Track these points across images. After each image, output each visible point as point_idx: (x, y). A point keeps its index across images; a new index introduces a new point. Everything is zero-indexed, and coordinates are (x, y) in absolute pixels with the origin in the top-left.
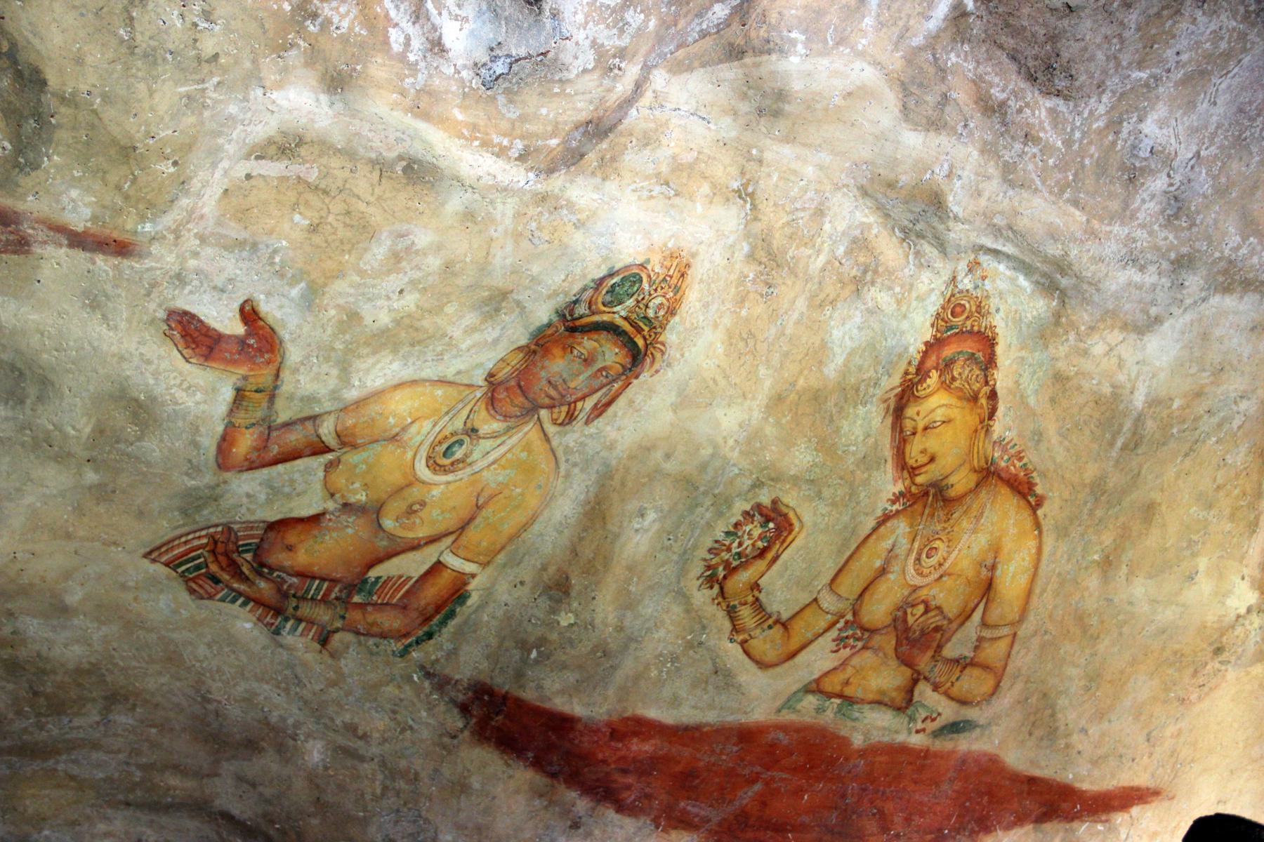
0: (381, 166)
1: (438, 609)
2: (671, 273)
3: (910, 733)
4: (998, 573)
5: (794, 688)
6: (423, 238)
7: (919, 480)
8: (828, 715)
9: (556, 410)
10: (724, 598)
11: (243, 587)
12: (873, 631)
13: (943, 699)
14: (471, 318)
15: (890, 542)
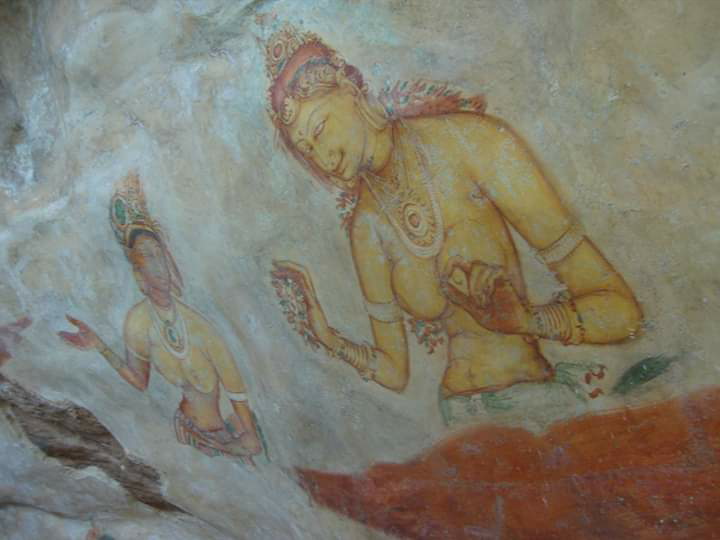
0: (35, 237)
3: (584, 400)
4: (493, 194)
5: (435, 397)
7: (348, 174)
8: (484, 417)
10: (331, 349)
12: (439, 318)
13: (587, 348)
15: (374, 235)
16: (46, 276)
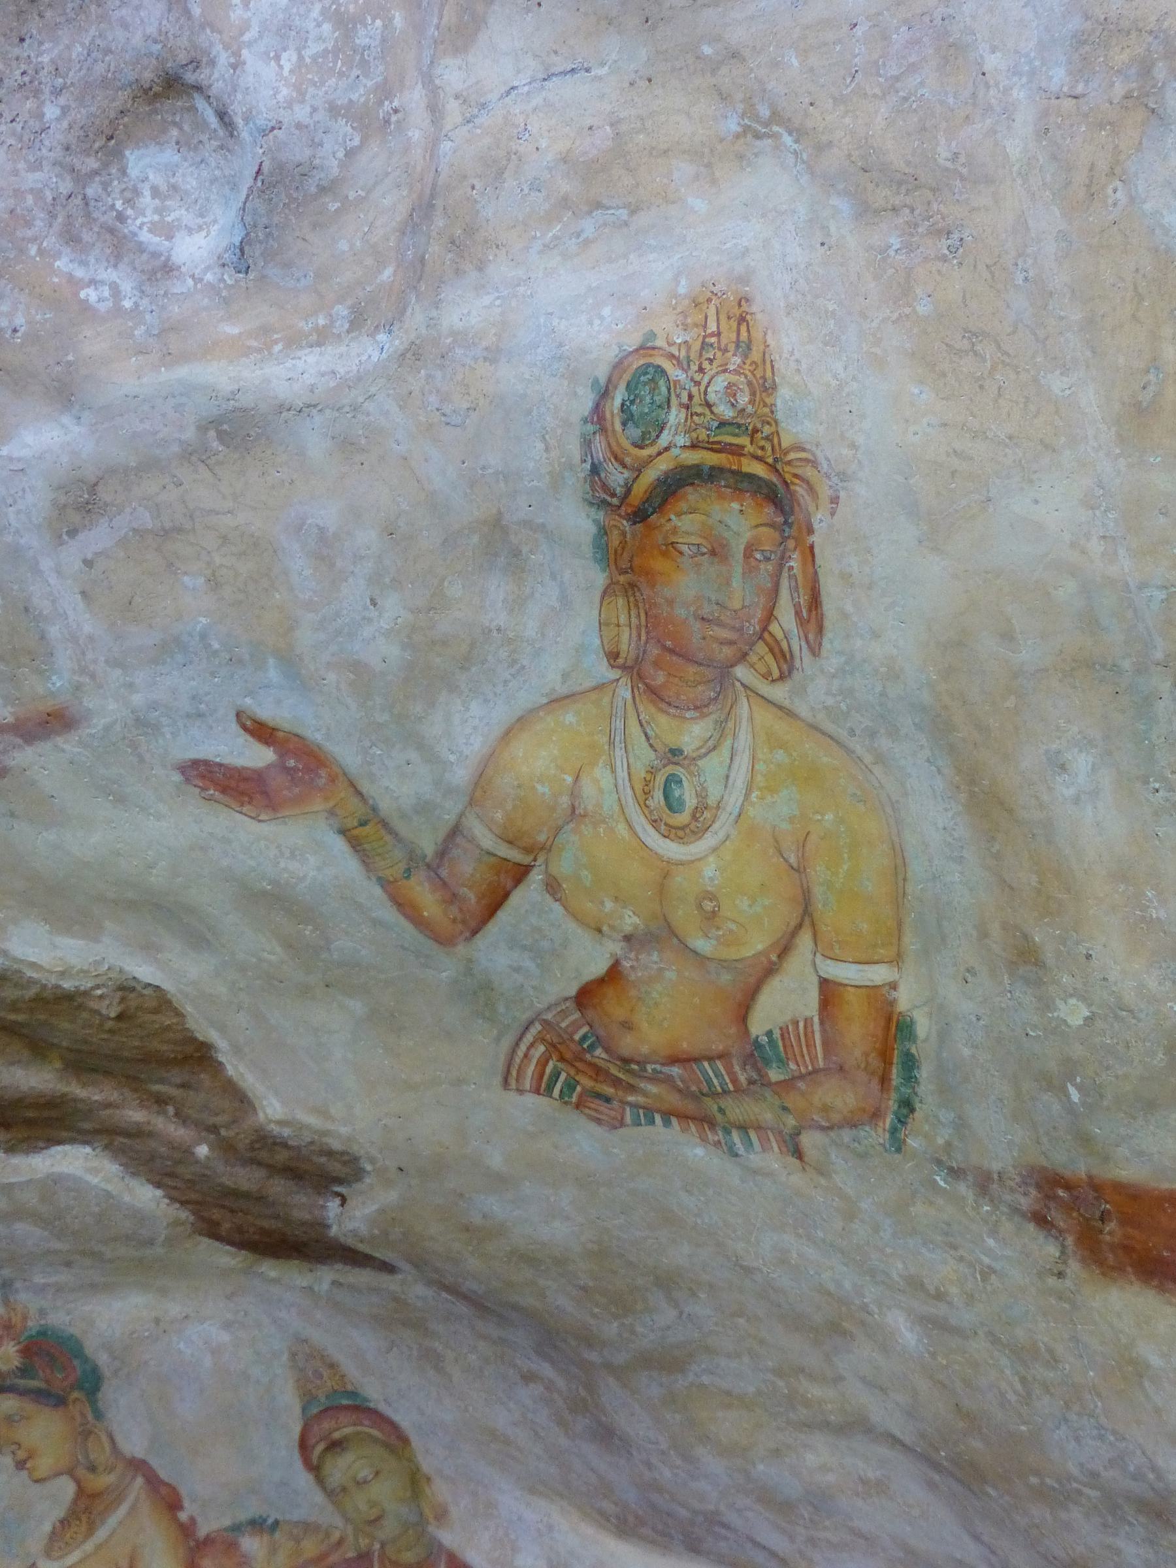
1: (885, 1057)
2: (712, 327)
6: (328, 514)
9: (753, 658)
11: (641, 1099)
14: (498, 588)
16: (194, 581)
